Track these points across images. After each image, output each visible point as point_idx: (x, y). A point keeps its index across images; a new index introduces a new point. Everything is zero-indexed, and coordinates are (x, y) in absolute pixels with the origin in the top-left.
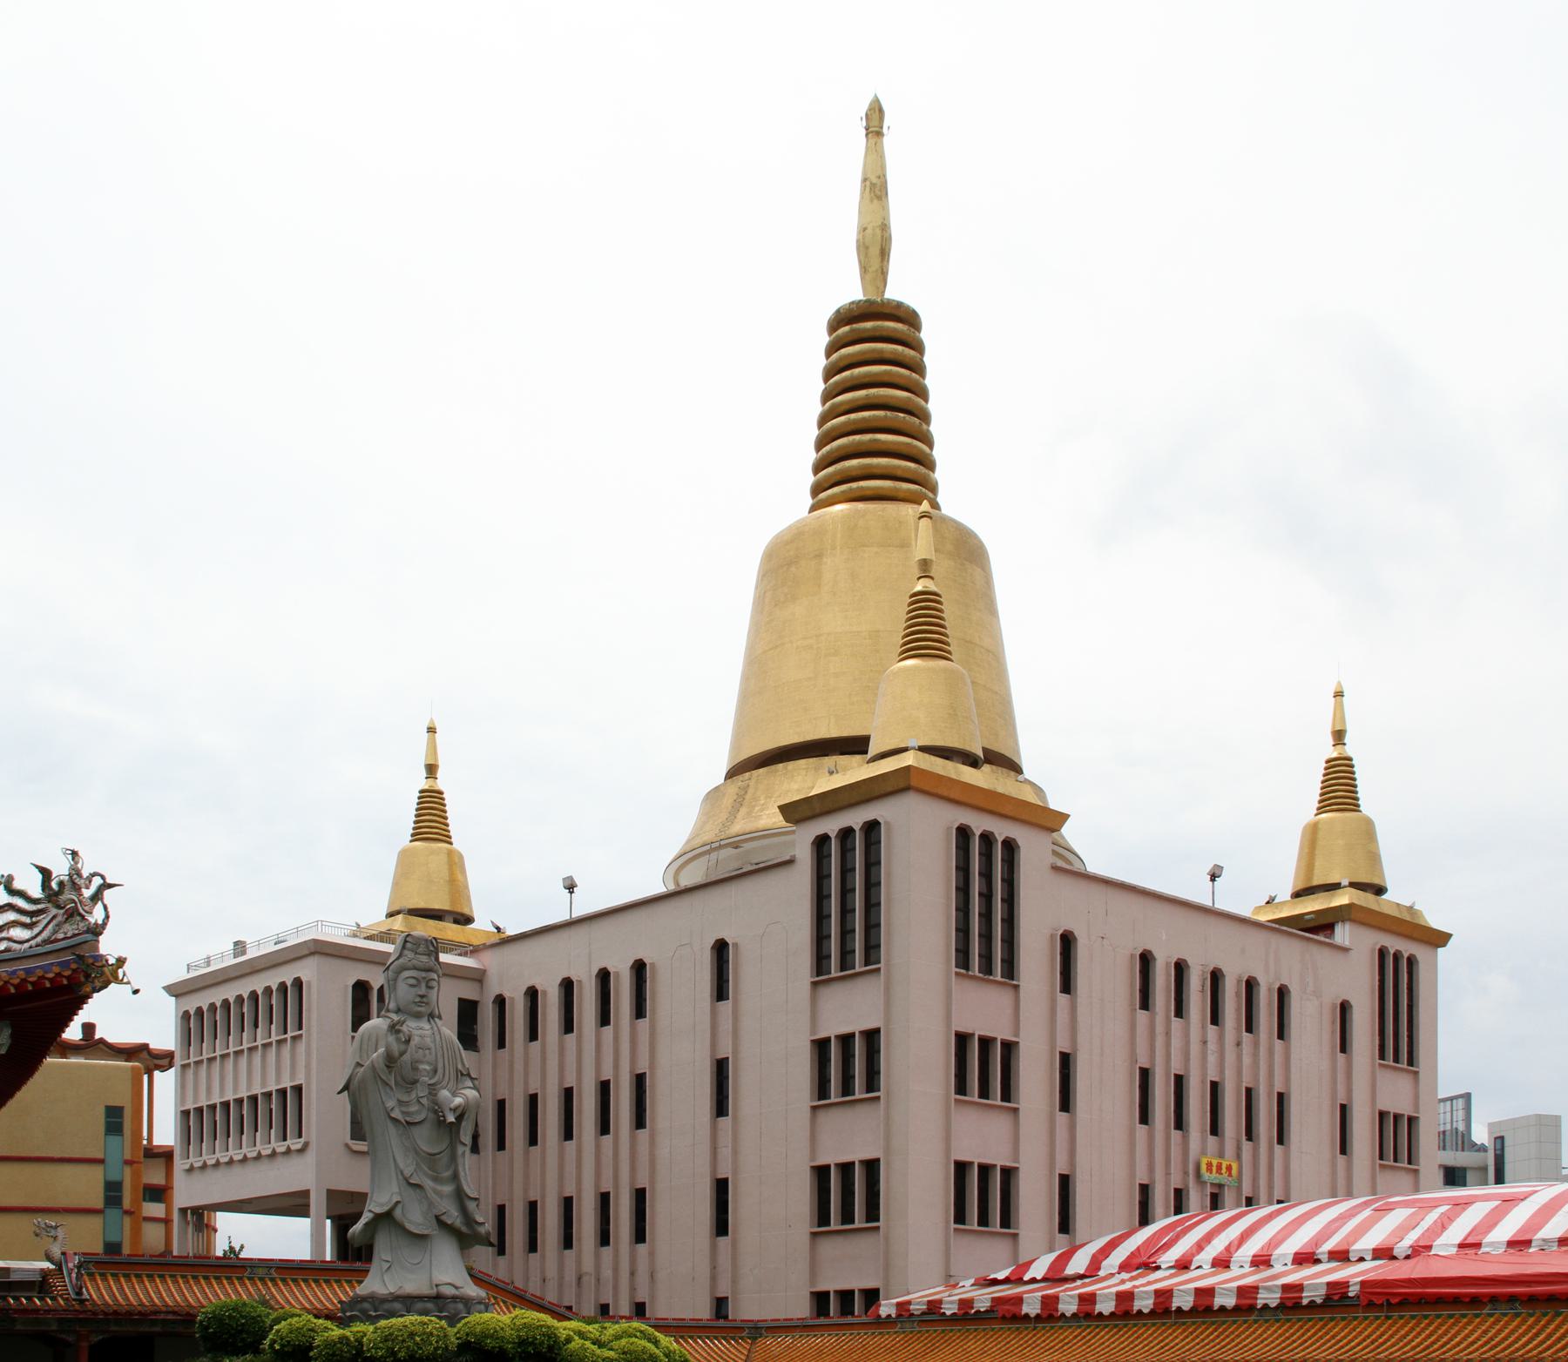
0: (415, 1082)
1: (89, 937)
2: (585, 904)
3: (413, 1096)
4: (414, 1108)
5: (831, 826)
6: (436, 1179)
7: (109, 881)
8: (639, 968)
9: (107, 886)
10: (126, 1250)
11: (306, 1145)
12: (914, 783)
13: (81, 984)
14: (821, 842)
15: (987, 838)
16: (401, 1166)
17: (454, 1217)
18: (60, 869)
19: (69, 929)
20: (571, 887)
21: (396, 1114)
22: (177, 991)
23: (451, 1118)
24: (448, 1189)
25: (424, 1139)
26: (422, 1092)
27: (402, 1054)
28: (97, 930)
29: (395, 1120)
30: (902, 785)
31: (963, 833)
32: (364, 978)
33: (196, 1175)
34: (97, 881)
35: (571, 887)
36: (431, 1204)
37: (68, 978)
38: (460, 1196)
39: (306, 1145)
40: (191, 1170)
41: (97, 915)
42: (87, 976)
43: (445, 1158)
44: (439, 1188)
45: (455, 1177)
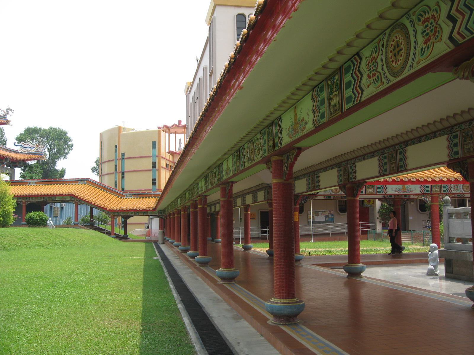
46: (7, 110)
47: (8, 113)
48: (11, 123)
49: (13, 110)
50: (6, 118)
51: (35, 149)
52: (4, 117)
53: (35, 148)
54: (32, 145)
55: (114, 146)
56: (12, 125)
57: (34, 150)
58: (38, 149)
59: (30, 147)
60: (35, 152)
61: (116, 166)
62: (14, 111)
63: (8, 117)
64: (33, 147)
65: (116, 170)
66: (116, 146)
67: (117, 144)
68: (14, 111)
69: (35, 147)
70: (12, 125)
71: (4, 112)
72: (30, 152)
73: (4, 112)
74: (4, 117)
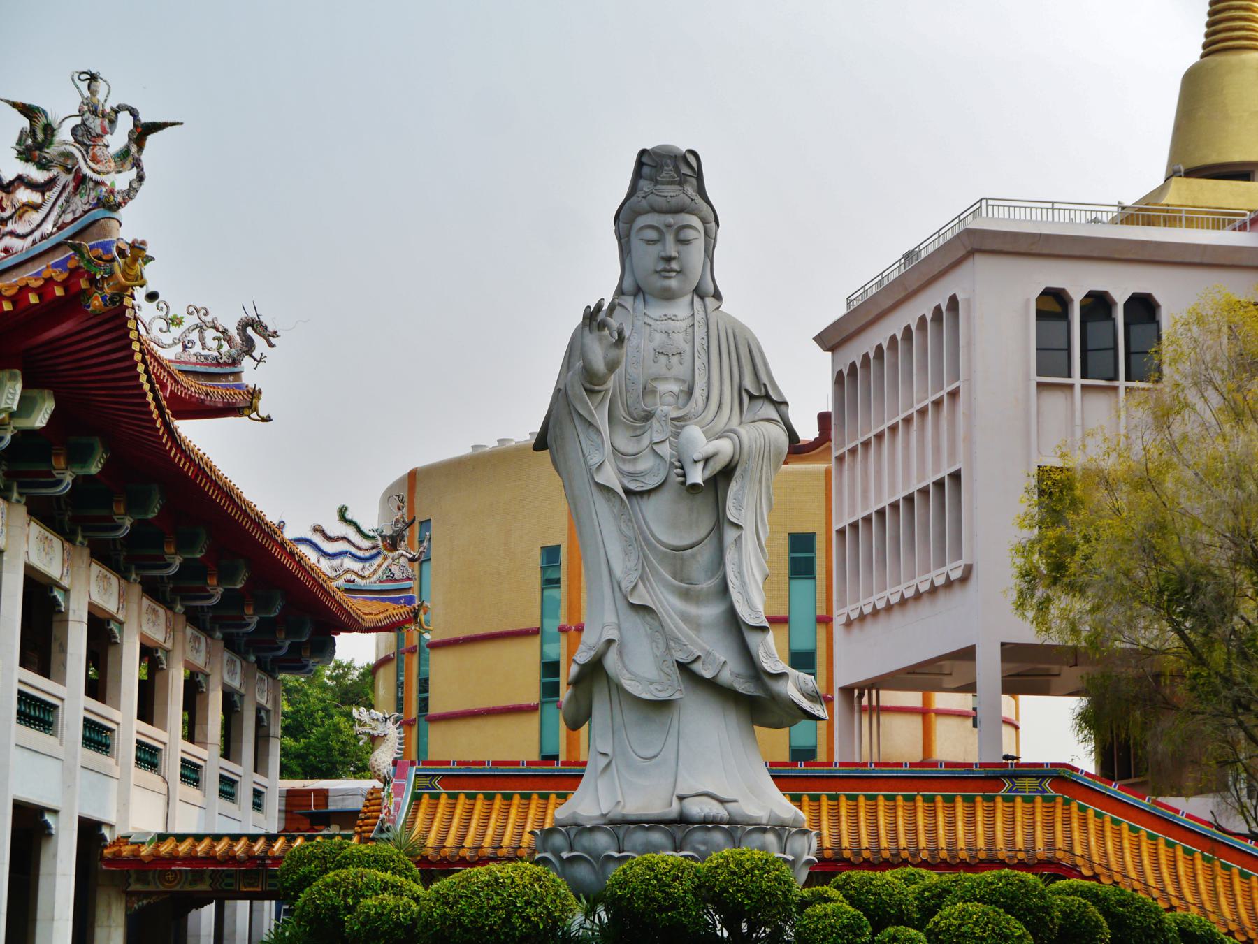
0: (648, 417)
1: (99, 213)
3: (645, 441)
4: (645, 464)
6: (686, 595)
7: (145, 118)
9: (142, 132)
10: (821, 756)
11: (969, 570)
13: (87, 294)
16: (618, 571)
18: (63, 107)
19: (79, 204)
21: (608, 476)
22: (831, 340)
24: (711, 612)
25: (663, 521)
26: (657, 431)
27: (612, 366)
28: (110, 204)
29: (605, 489)
32: (1099, 287)
33: (856, 630)
34: (125, 123)
36: (669, 640)
37: (63, 284)
38: (734, 625)
39: (969, 570)
40: (849, 624)
41: (121, 181)
42: (92, 280)
43: (704, 555)
44: (692, 610)
45: (724, 590)
47: (249, 346)
48: (264, 408)
49: (271, 329)
50: (237, 375)
51: (380, 566)
52: (225, 369)
53: (379, 560)
54: (366, 544)
55: (537, 556)
56: (267, 419)
57: (375, 571)
58: (395, 569)
59: (353, 556)
60: (378, 586)
62: (275, 335)
63: (250, 374)
64: (367, 554)
65: (550, 690)
66: (551, 554)
67: (559, 537)
68: (275, 335)
69: (379, 554)
70: (267, 419)
71: (229, 340)
72: (358, 580)
73: (229, 340)
74: (225, 369)
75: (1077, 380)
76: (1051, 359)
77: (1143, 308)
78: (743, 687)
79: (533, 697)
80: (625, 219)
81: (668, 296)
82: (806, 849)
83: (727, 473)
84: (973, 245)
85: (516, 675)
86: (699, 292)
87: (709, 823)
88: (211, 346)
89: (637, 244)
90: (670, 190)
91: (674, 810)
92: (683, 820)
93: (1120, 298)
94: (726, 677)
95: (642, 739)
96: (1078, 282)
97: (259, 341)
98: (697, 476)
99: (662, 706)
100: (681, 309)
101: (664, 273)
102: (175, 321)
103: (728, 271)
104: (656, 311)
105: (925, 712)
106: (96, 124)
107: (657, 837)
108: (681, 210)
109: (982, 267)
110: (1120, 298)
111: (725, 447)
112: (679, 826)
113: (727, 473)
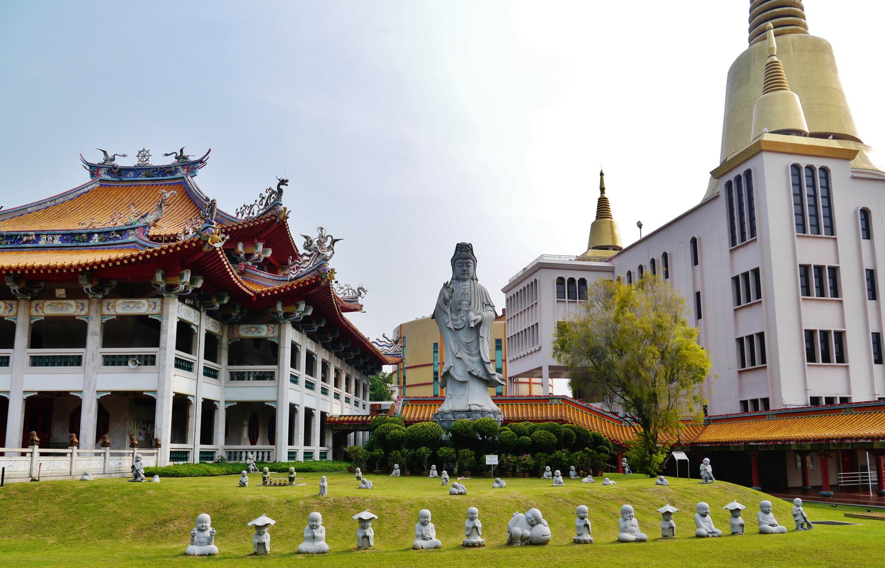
2: (646, 231)
4: (459, 322)
5: (731, 177)
6: (470, 355)
8: (665, 256)
9: (334, 241)
11: (540, 348)
12: (763, 147)
13: (320, 282)
14: (729, 185)
15: (810, 168)
17: (479, 371)
18: (314, 236)
19: (318, 260)
20: (640, 225)
21: (450, 325)
23: (472, 325)
24: (476, 359)
25: (464, 336)
26: (462, 314)
27: (451, 298)
28: (326, 260)
29: (450, 328)
30: (758, 150)
31: (796, 167)
34: (330, 239)
35: (640, 225)
36: (466, 366)
38: (482, 362)
39: (540, 348)
41: (329, 254)
43: (474, 345)
44: (472, 358)
45: (479, 353)
46: (359, 289)
47: (360, 293)
61: (436, 373)
63: (360, 301)
65: (436, 379)
66: (436, 345)
67: (438, 341)
75: (567, 299)
76: (560, 294)
77: (583, 282)
78: (484, 377)
79: (432, 381)
80: (454, 261)
81: (465, 280)
82: (501, 418)
83: (480, 324)
84: (541, 266)
85: (427, 375)
86: (472, 279)
87: (476, 411)
88: (351, 294)
89: (456, 267)
90: (465, 253)
91: (468, 408)
92: (470, 411)
93: (577, 279)
94: (480, 375)
95: (459, 391)
96: (567, 275)
97: (363, 293)
98: (472, 325)
99: (464, 382)
100: (468, 283)
101: (464, 274)
102: (342, 288)
103: (478, 274)
104: (461, 284)
105: (530, 383)
106: (322, 240)
107: (463, 415)
108: (468, 258)
109: (542, 271)
110: (577, 279)
111: (479, 317)
112: (469, 412)
113: (480, 324)
